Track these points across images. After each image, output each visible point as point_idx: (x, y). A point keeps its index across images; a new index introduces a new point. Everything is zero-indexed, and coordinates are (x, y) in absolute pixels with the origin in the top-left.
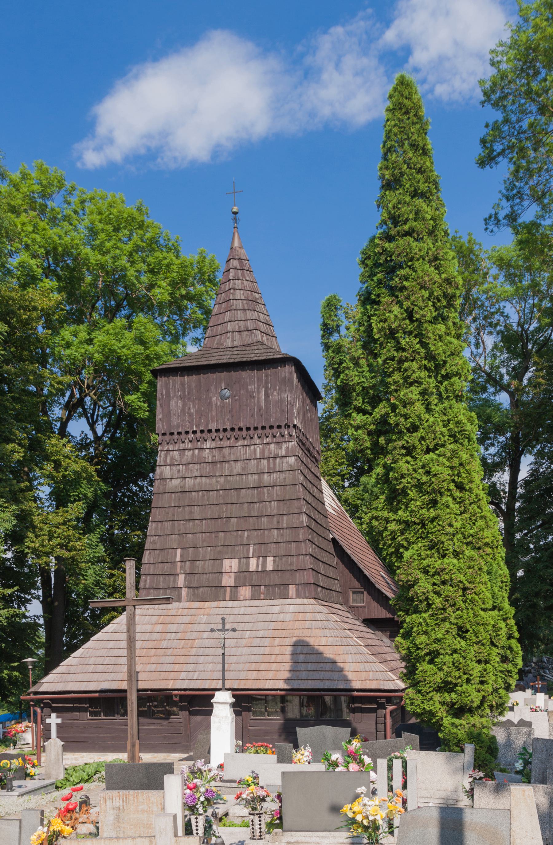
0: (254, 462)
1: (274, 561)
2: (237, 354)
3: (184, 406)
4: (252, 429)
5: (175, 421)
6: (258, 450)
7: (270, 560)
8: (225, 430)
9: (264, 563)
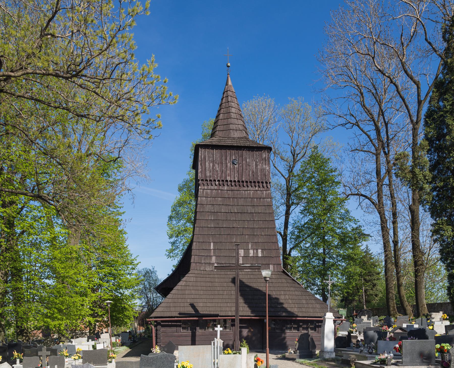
0: (250, 200)
1: (262, 252)
2: (236, 142)
3: (214, 166)
4: (249, 182)
5: (208, 174)
6: (251, 193)
7: (260, 251)
8: (235, 181)
9: (257, 252)
